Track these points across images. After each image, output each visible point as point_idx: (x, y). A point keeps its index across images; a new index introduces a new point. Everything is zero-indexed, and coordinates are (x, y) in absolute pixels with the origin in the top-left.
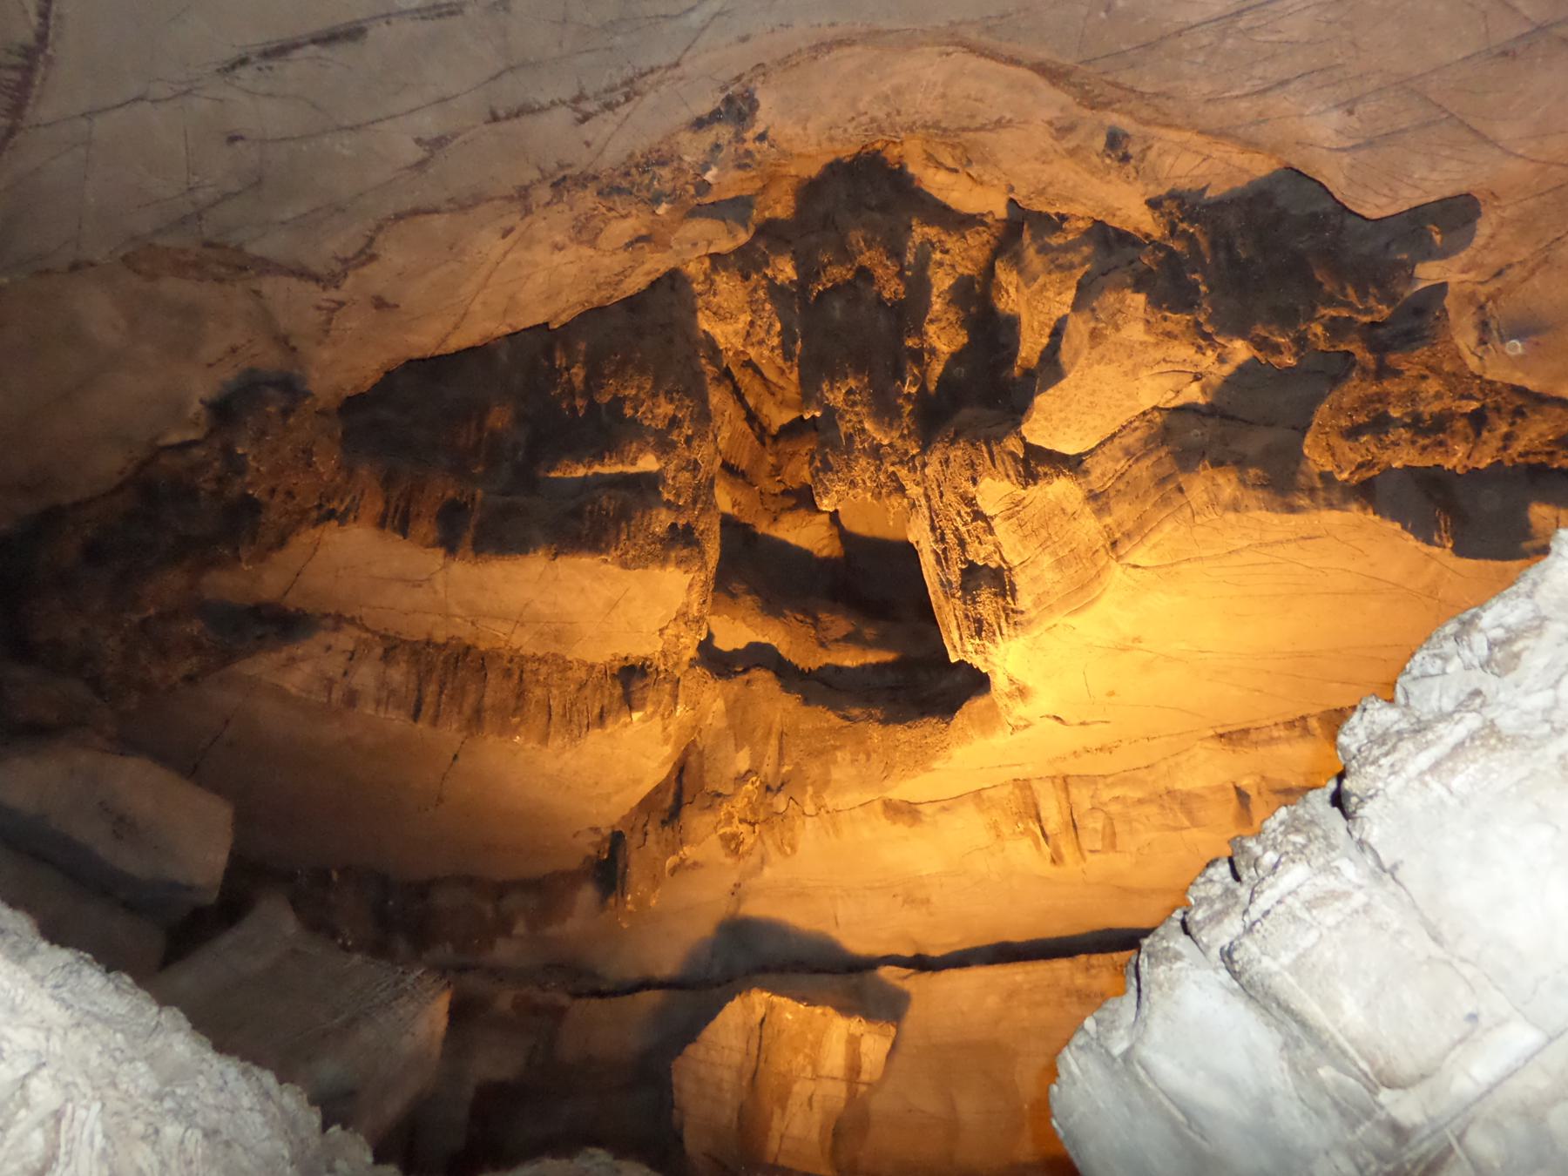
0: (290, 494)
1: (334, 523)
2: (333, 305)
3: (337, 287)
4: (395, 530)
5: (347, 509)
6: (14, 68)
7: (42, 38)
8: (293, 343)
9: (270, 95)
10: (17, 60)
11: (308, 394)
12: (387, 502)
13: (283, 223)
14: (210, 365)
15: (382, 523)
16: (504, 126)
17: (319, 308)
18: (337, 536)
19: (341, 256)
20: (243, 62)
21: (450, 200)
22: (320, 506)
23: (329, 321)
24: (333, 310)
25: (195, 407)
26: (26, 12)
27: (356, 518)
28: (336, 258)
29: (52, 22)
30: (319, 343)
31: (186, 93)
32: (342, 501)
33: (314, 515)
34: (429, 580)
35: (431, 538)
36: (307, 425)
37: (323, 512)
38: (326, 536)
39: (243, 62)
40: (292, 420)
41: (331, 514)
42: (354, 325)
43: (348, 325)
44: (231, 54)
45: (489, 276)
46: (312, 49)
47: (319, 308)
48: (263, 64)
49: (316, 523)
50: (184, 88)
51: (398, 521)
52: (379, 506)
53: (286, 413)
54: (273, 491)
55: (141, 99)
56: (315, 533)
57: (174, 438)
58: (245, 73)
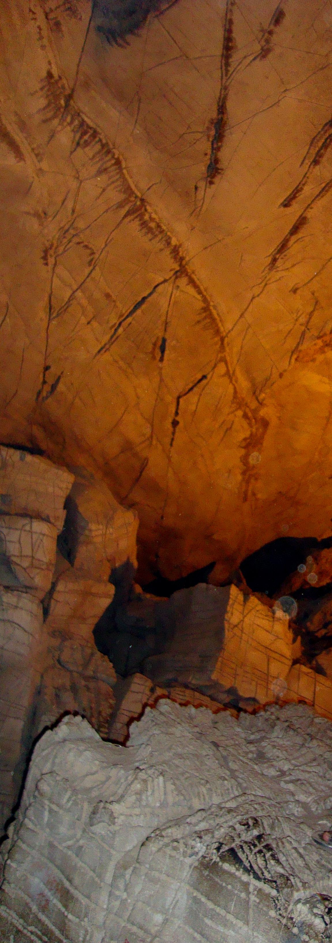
6: (205, 318)
7: (205, 300)
9: (293, 266)
10: (204, 315)
20: (275, 260)
26: (194, 297)
29: (205, 293)
31: (266, 284)
39: (275, 260)
44: (270, 259)
46: (294, 238)
48: (282, 256)
50: (263, 284)
55: (253, 298)
58: (279, 263)
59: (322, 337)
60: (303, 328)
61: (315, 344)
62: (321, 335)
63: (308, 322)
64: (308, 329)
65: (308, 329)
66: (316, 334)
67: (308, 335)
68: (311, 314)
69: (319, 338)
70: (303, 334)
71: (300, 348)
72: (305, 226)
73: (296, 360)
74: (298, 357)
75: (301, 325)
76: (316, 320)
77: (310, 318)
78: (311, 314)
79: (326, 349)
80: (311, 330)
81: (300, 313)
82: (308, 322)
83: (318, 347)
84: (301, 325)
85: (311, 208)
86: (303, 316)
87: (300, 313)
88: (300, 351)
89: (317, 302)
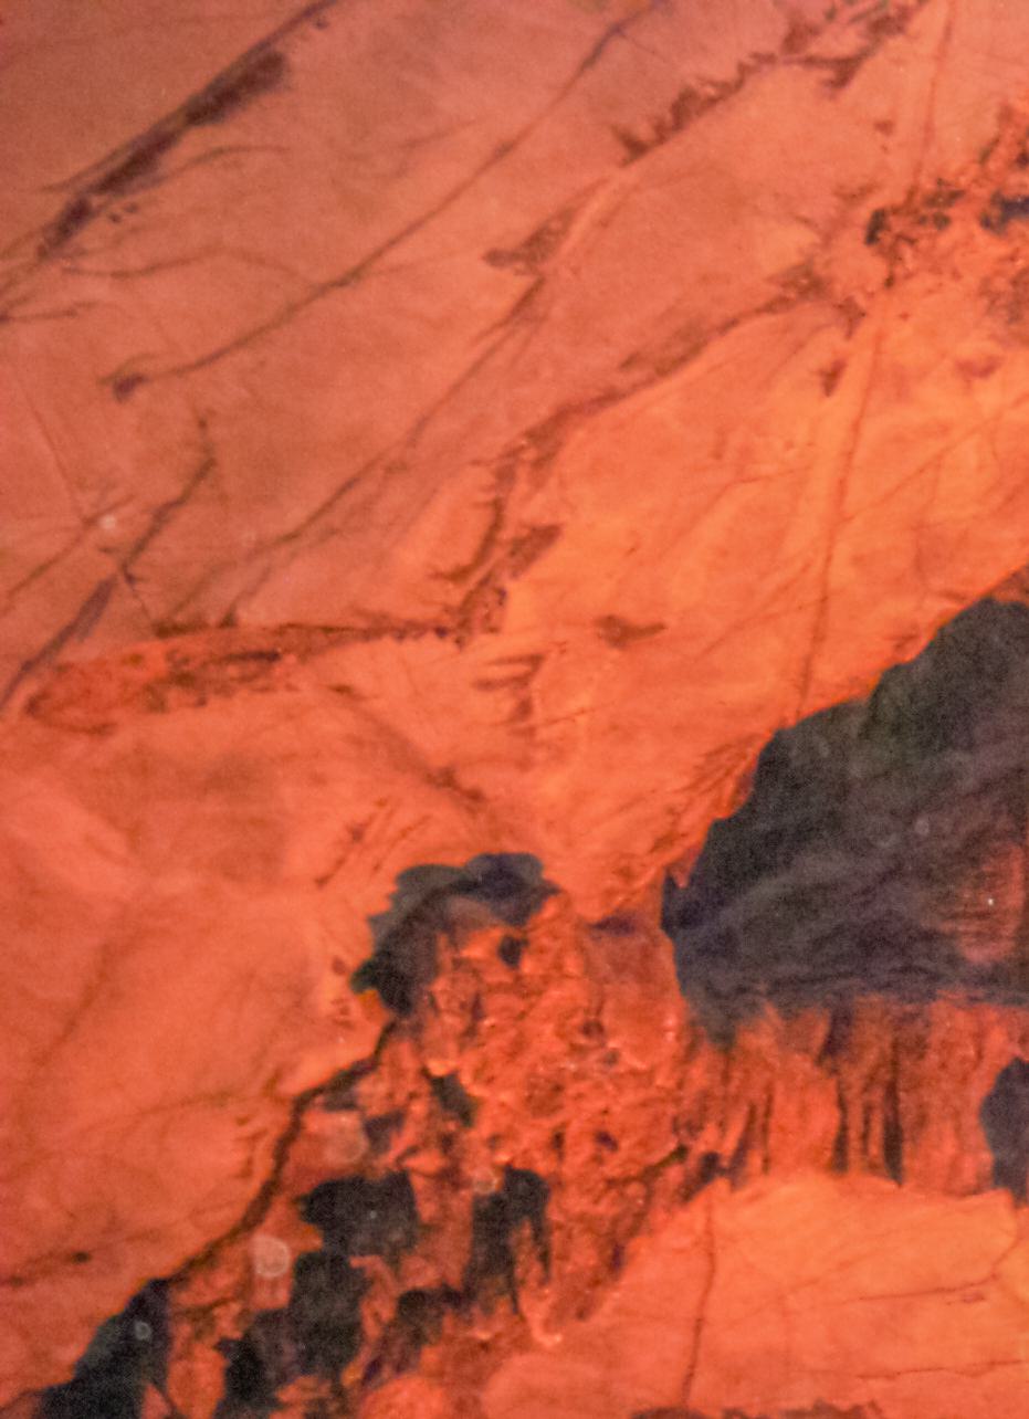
0: (605, 1139)
1: (720, 1185)
2: (521, 669)
3: (493, 630)
4: (873, 1168)
5: (743, 1147)
8: (468, 780)
11: (549, 891)
12: (842, 1104)
13: (291, 537)
14: (322, 882)
15: (838, 1159)
16: (668, 156)
17: (486, 685)
18: (747, 1215)
19: (446, 566)
21: (629, 362)
22: (681, 1152)
23: (525, 709)
24: (522, 681)
25: (330, 990)
27: (767, 1161)
28: (438, 575)
30: (524, 764)
32: (722, 1125)
33: (674, 1174)
34: (994, 1277)
35: (968, 1176)
36: (572, 965)
37: (692, 1163)
38: (722, 1219)
40: (528, 966)
41: (711, 1166)
42: (584, 699)
43: (573, 705)
45: (841, 488)
47: (486, 685)
49: (687, 1193)
51: (883, 1145)
52: (824, 1120)
53: (510, 952)
54: (557, 1141)
56: (694, 1215)
57: (313, 1069)
59: (178, 630)
60: (108, 567)
61: (136, 659)
62: (180, 618)
63: (140, 546)
64: (130, 579)
65: (130, 579)
66: (159, 611)
67: (121, 604)
68: (162, 515)
69: (163, 630)
70: (100, 597)
71: (69, 654)
72: (267, 99)
73: (32, 707)
74: (44, 695)
75: (106, 550)
76: (171, 546)
77: (153, 532)
78: (162, 515)
79: (173, 695)
80: (139, 587)
81: (113, 496)
82: (140, 546)
83: (140, 675)
84: (106, 550)
85: (321, 25)
86: (127, 510)
87: (113, 496)
88: (63, 670)
89: (205, 469)
